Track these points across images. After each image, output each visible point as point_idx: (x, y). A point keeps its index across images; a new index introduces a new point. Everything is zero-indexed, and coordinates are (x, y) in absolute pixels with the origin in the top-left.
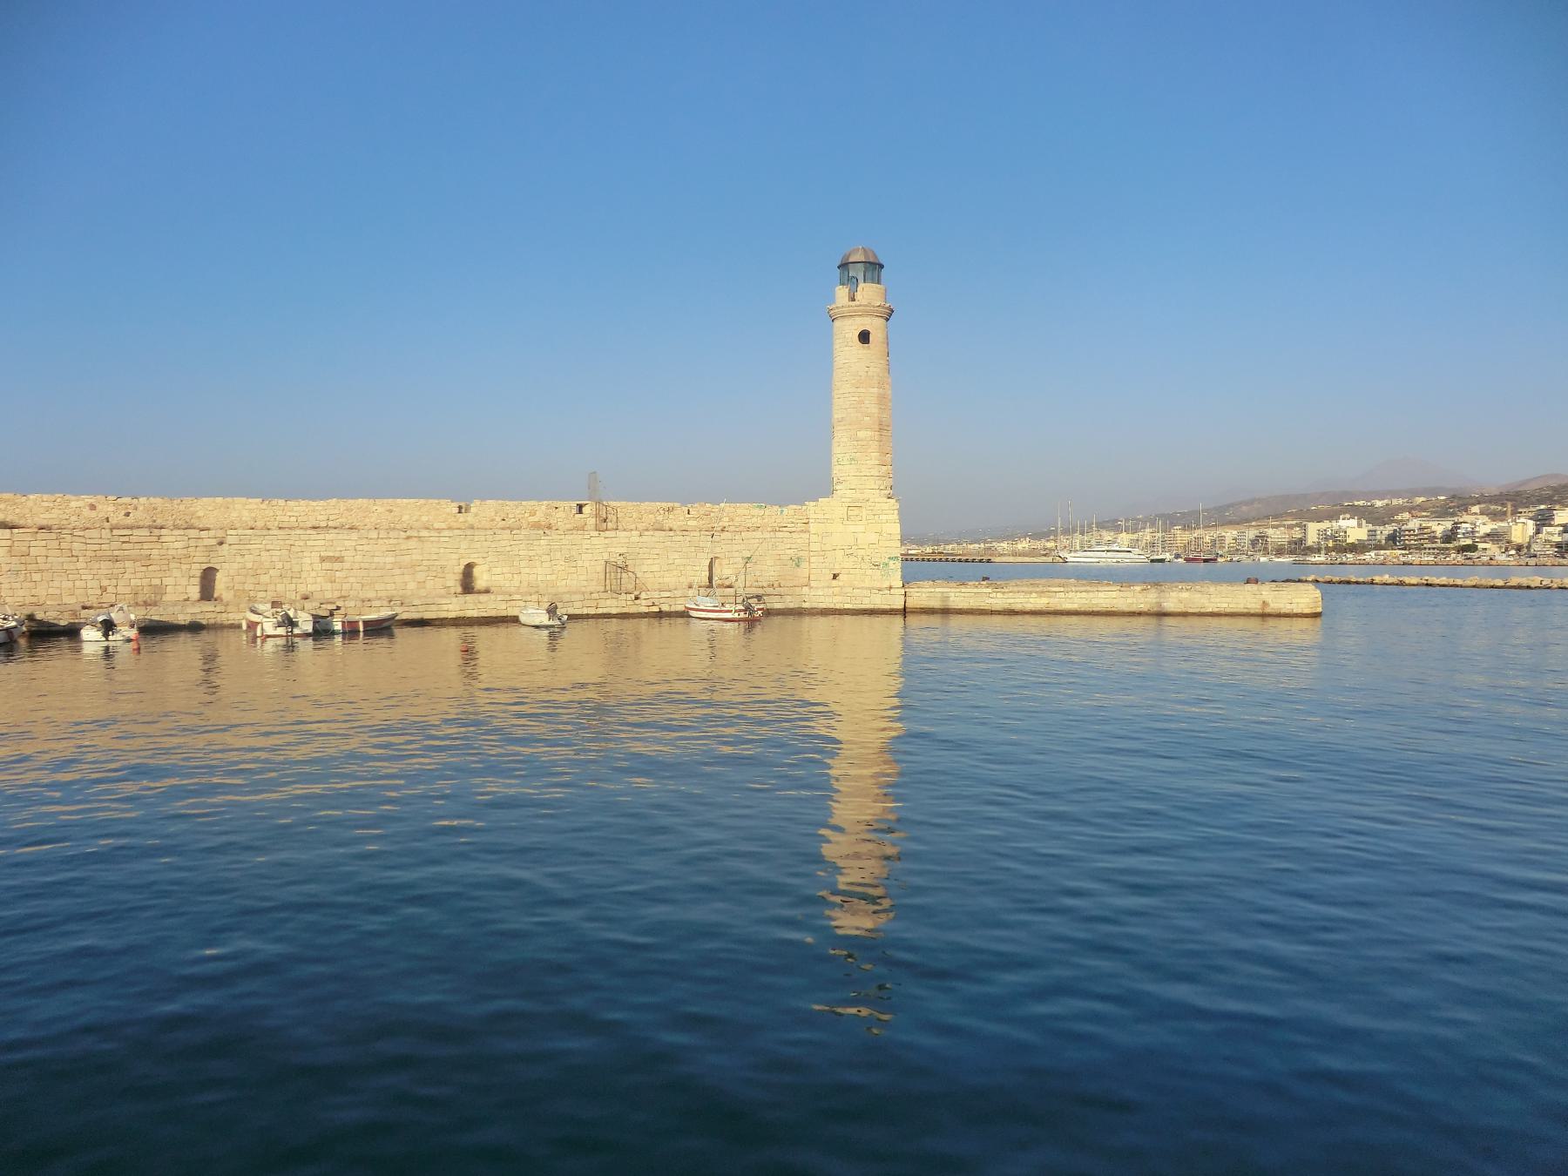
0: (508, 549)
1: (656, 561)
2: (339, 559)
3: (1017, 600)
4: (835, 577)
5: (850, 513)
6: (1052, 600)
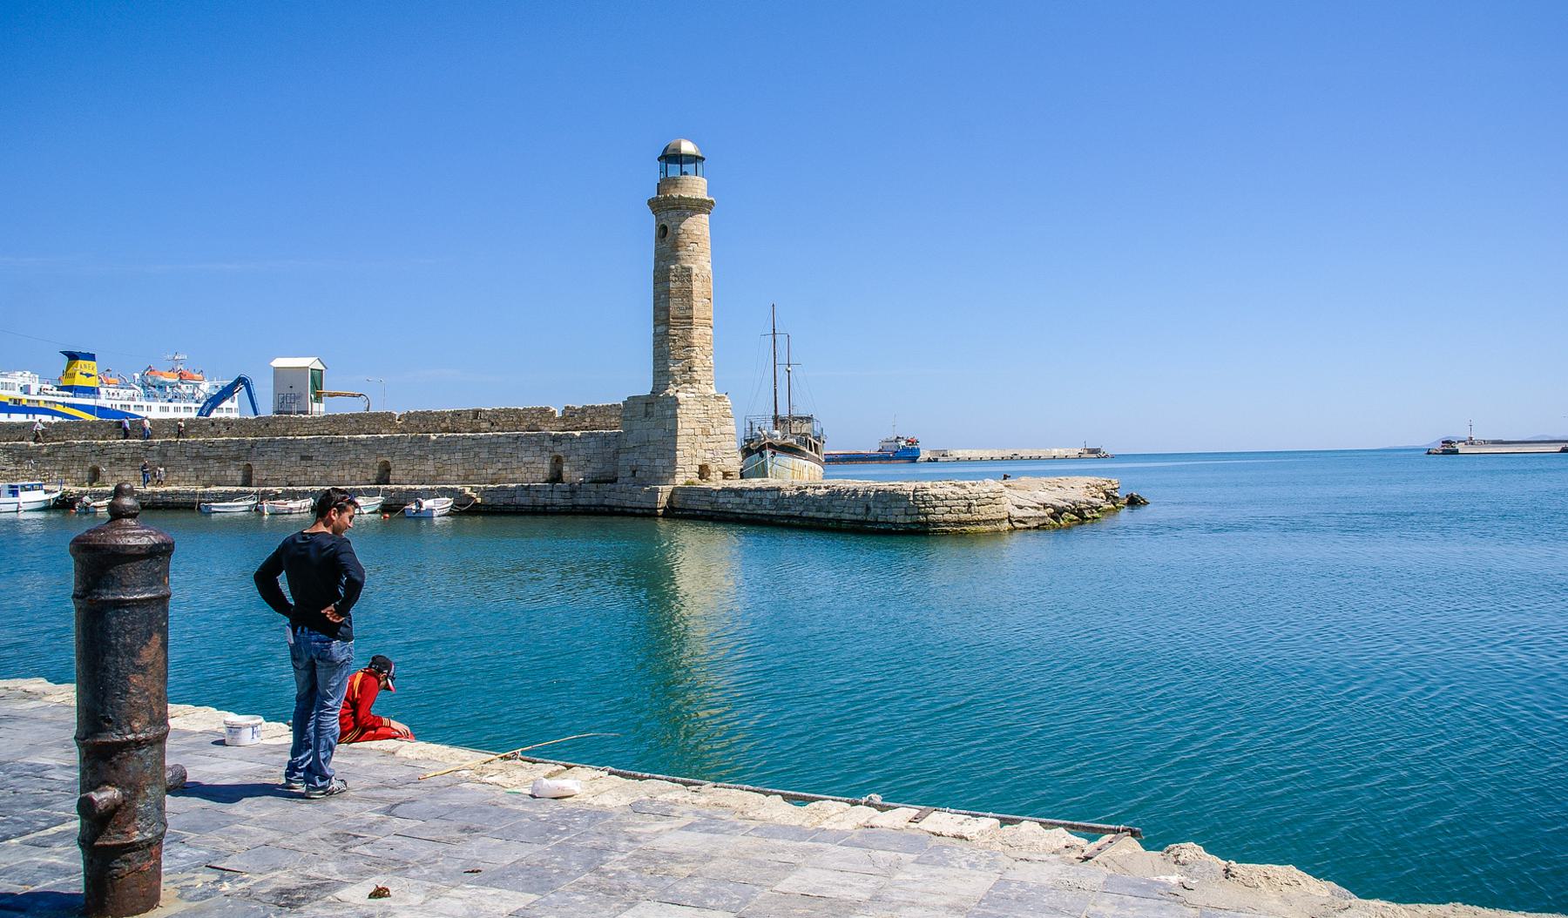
2: (310, 458)
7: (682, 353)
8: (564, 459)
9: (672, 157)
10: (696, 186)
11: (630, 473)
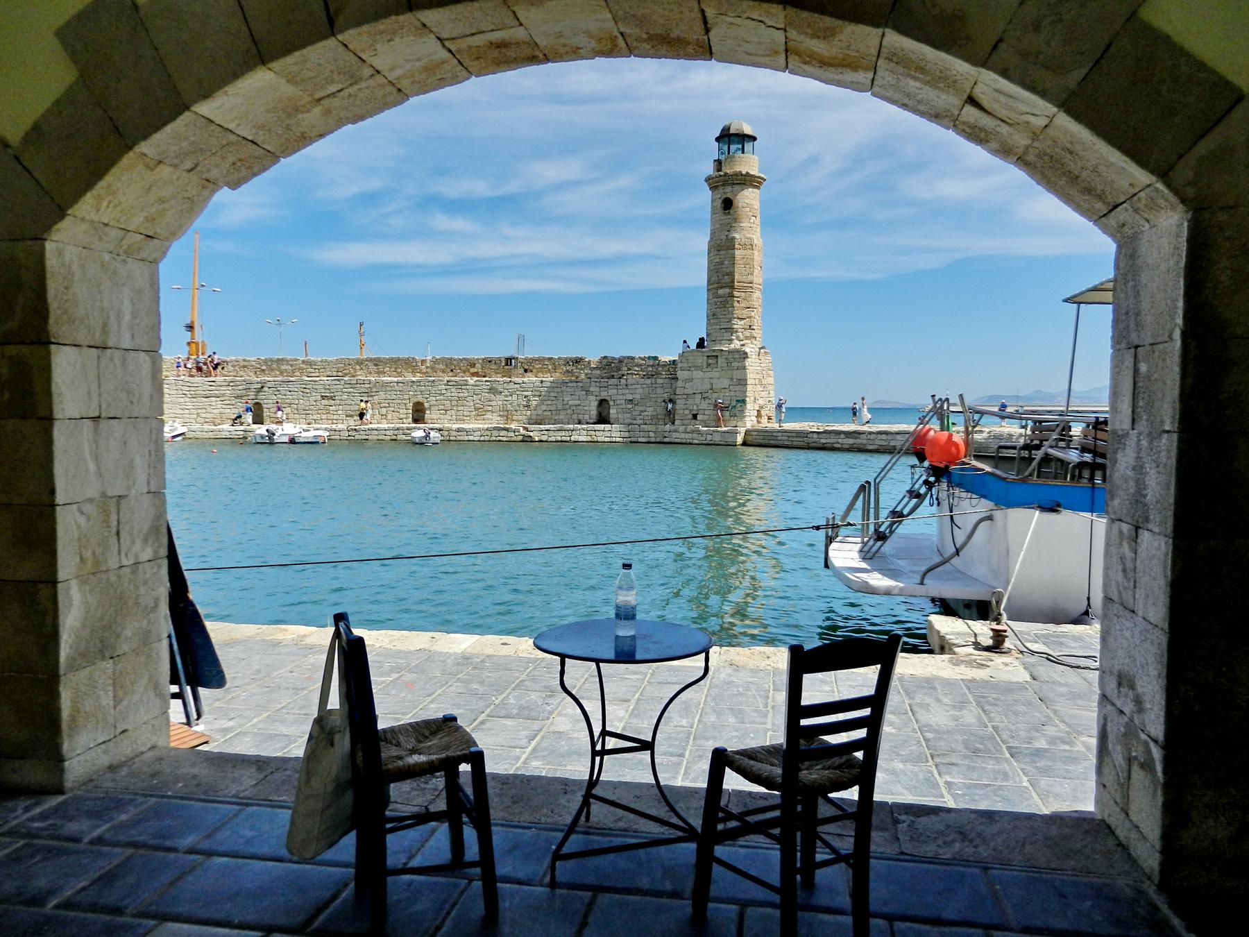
0: (445, 391)
1: (554, 402)
2: (332, 398)
3: (828, 441)
4: (695, 417)
5: (710, 361)
6: (857, 441)
7: (746, 313)
8: (611, 403)
9: (728, 137)
10: (749, 163)
11: (691, 416)
